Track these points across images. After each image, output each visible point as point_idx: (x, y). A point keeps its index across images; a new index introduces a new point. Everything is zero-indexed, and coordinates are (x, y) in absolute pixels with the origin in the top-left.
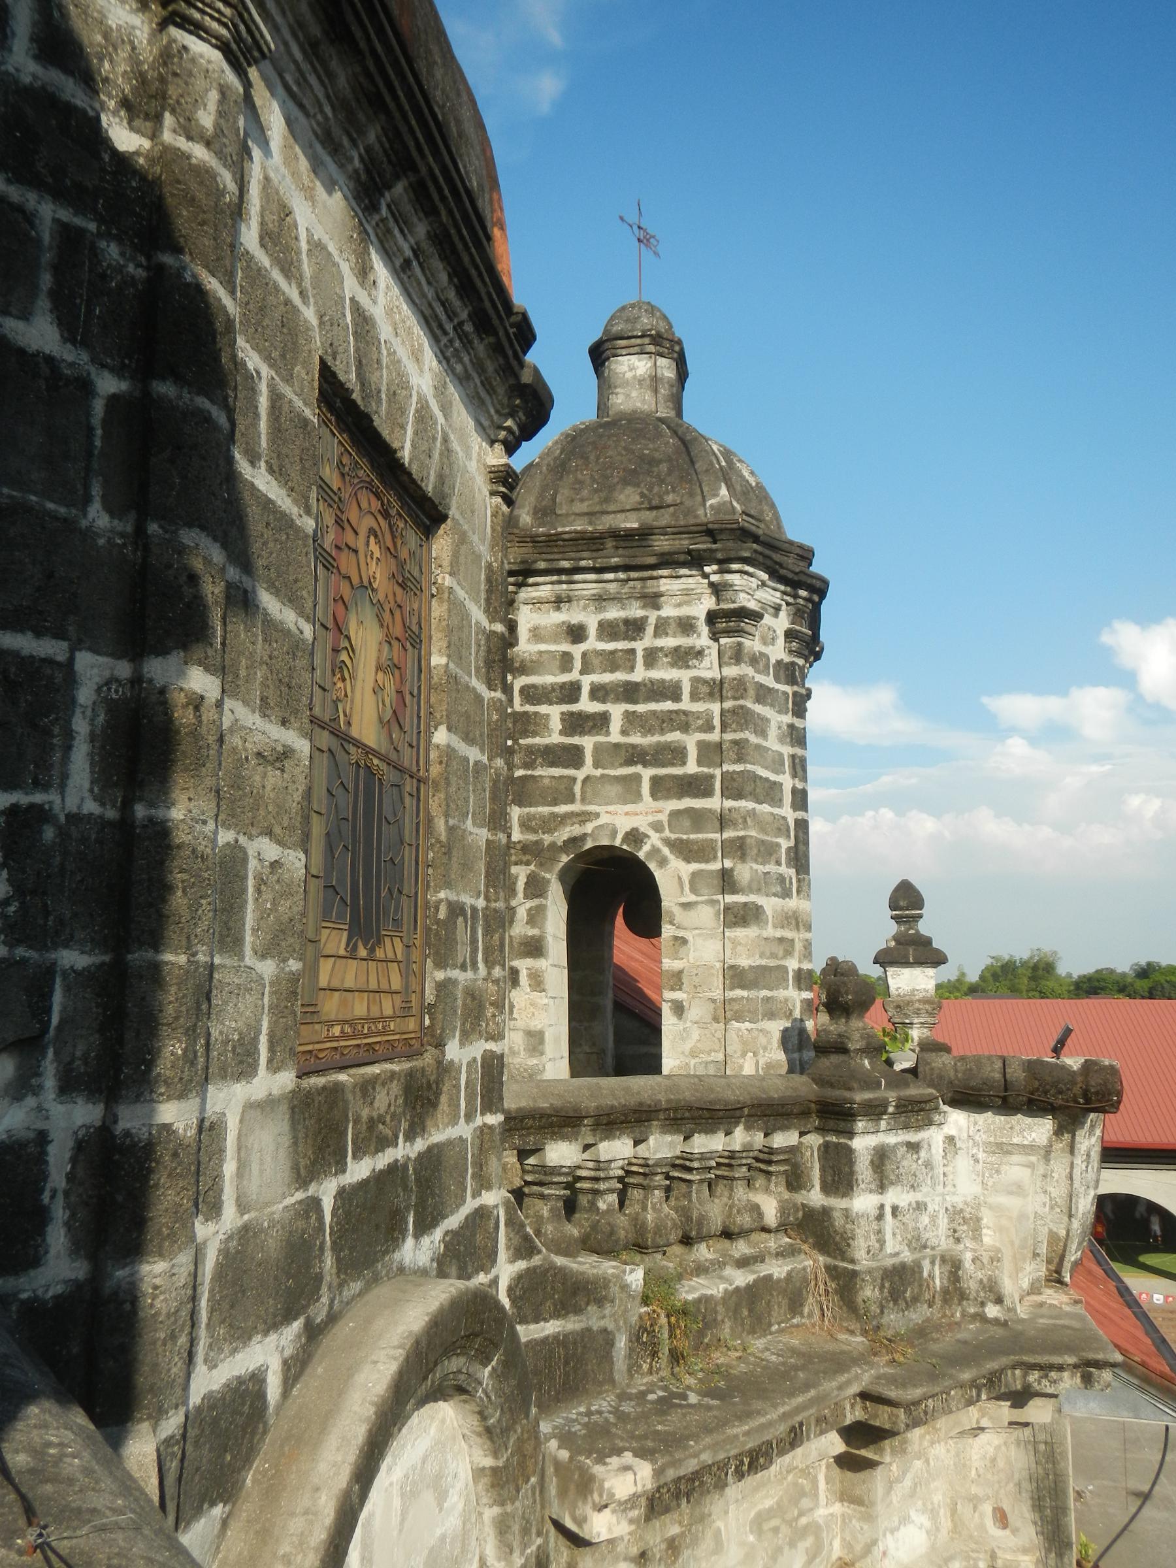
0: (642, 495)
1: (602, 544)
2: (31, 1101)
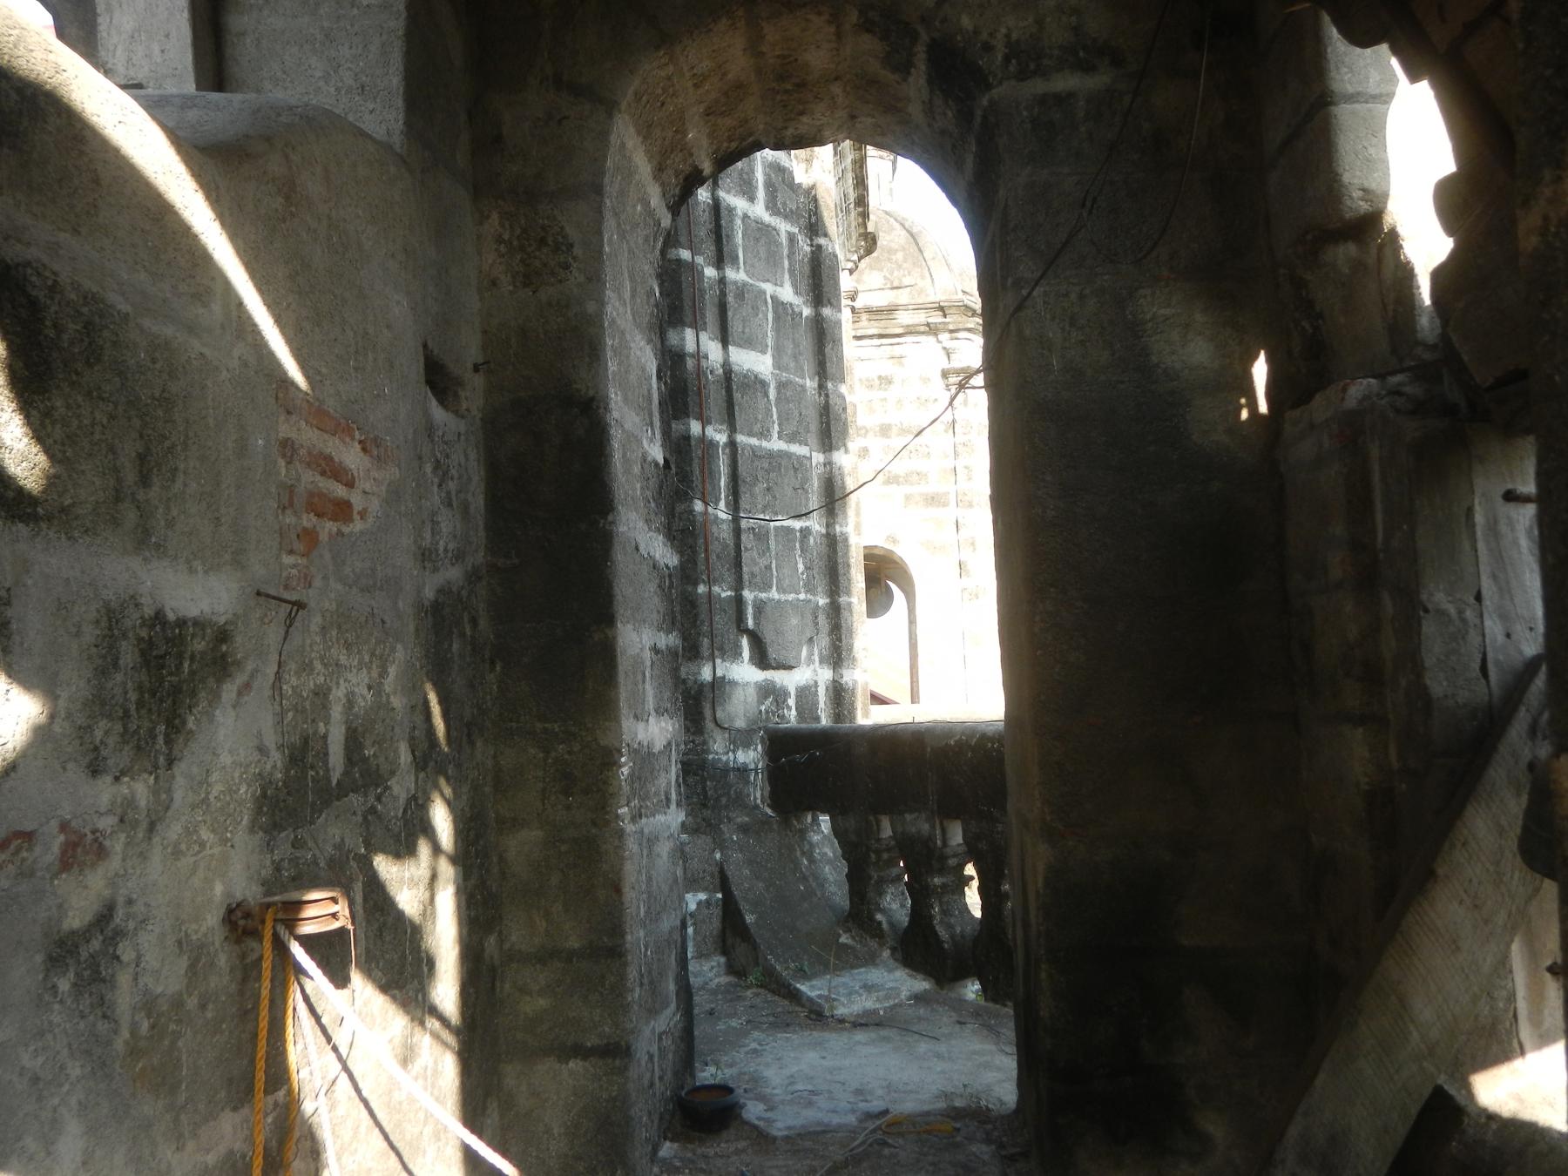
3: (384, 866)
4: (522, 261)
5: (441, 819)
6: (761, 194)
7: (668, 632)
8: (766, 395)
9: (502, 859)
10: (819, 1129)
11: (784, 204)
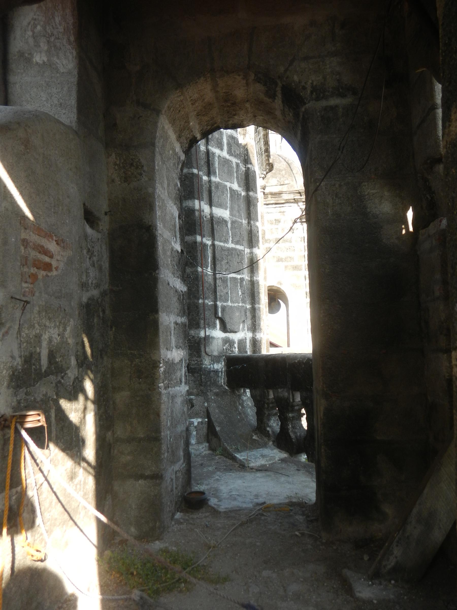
0: (278, 181)
1: (267, 196)
2: (244, 332)
3: (64, 404)
4: (124, 172)
5: (89, 386)
6: (225, 147)
7: (182, 317)
8: (227, 226)
9: (114, 403)
10: (238, 509)
11: (235, 151)
